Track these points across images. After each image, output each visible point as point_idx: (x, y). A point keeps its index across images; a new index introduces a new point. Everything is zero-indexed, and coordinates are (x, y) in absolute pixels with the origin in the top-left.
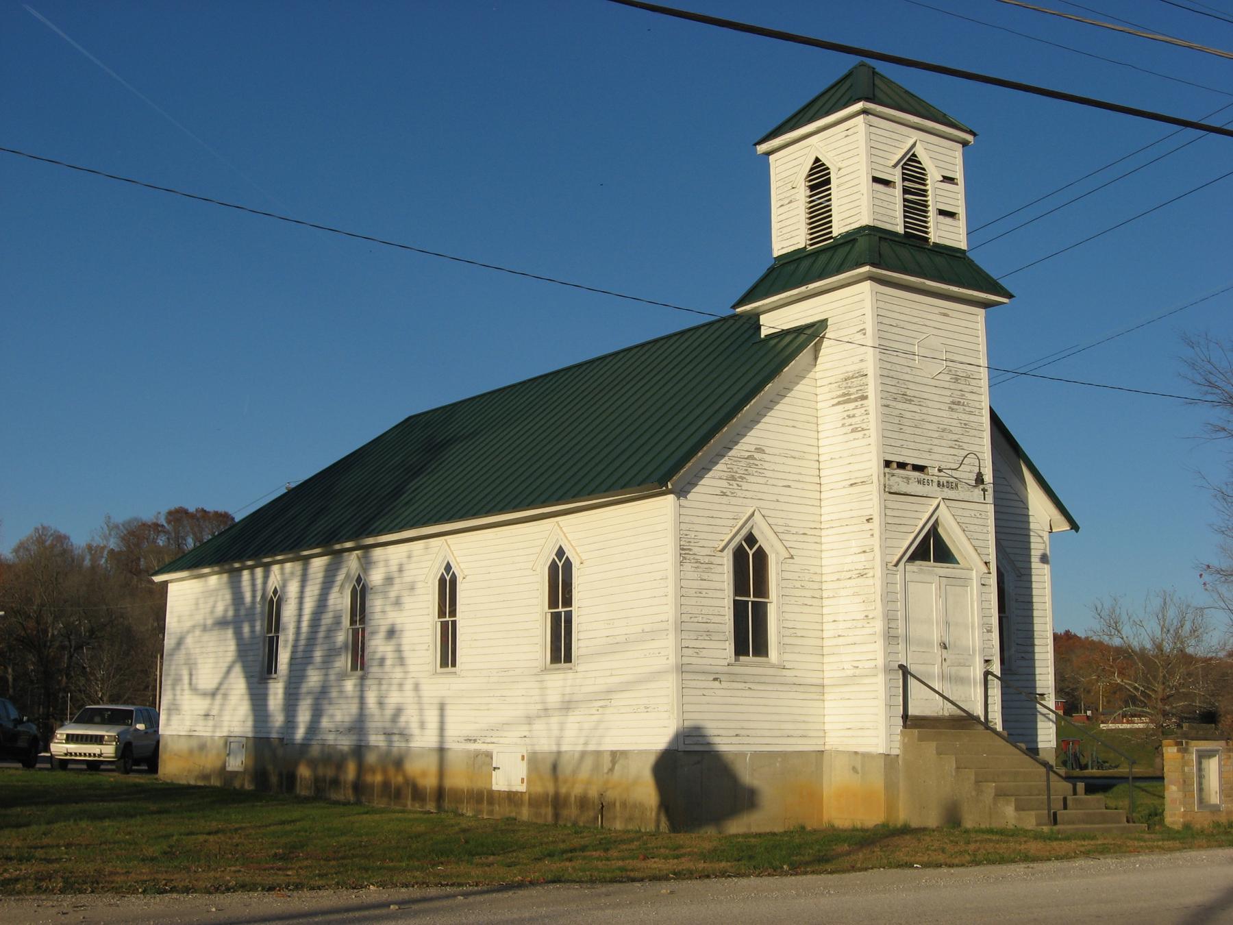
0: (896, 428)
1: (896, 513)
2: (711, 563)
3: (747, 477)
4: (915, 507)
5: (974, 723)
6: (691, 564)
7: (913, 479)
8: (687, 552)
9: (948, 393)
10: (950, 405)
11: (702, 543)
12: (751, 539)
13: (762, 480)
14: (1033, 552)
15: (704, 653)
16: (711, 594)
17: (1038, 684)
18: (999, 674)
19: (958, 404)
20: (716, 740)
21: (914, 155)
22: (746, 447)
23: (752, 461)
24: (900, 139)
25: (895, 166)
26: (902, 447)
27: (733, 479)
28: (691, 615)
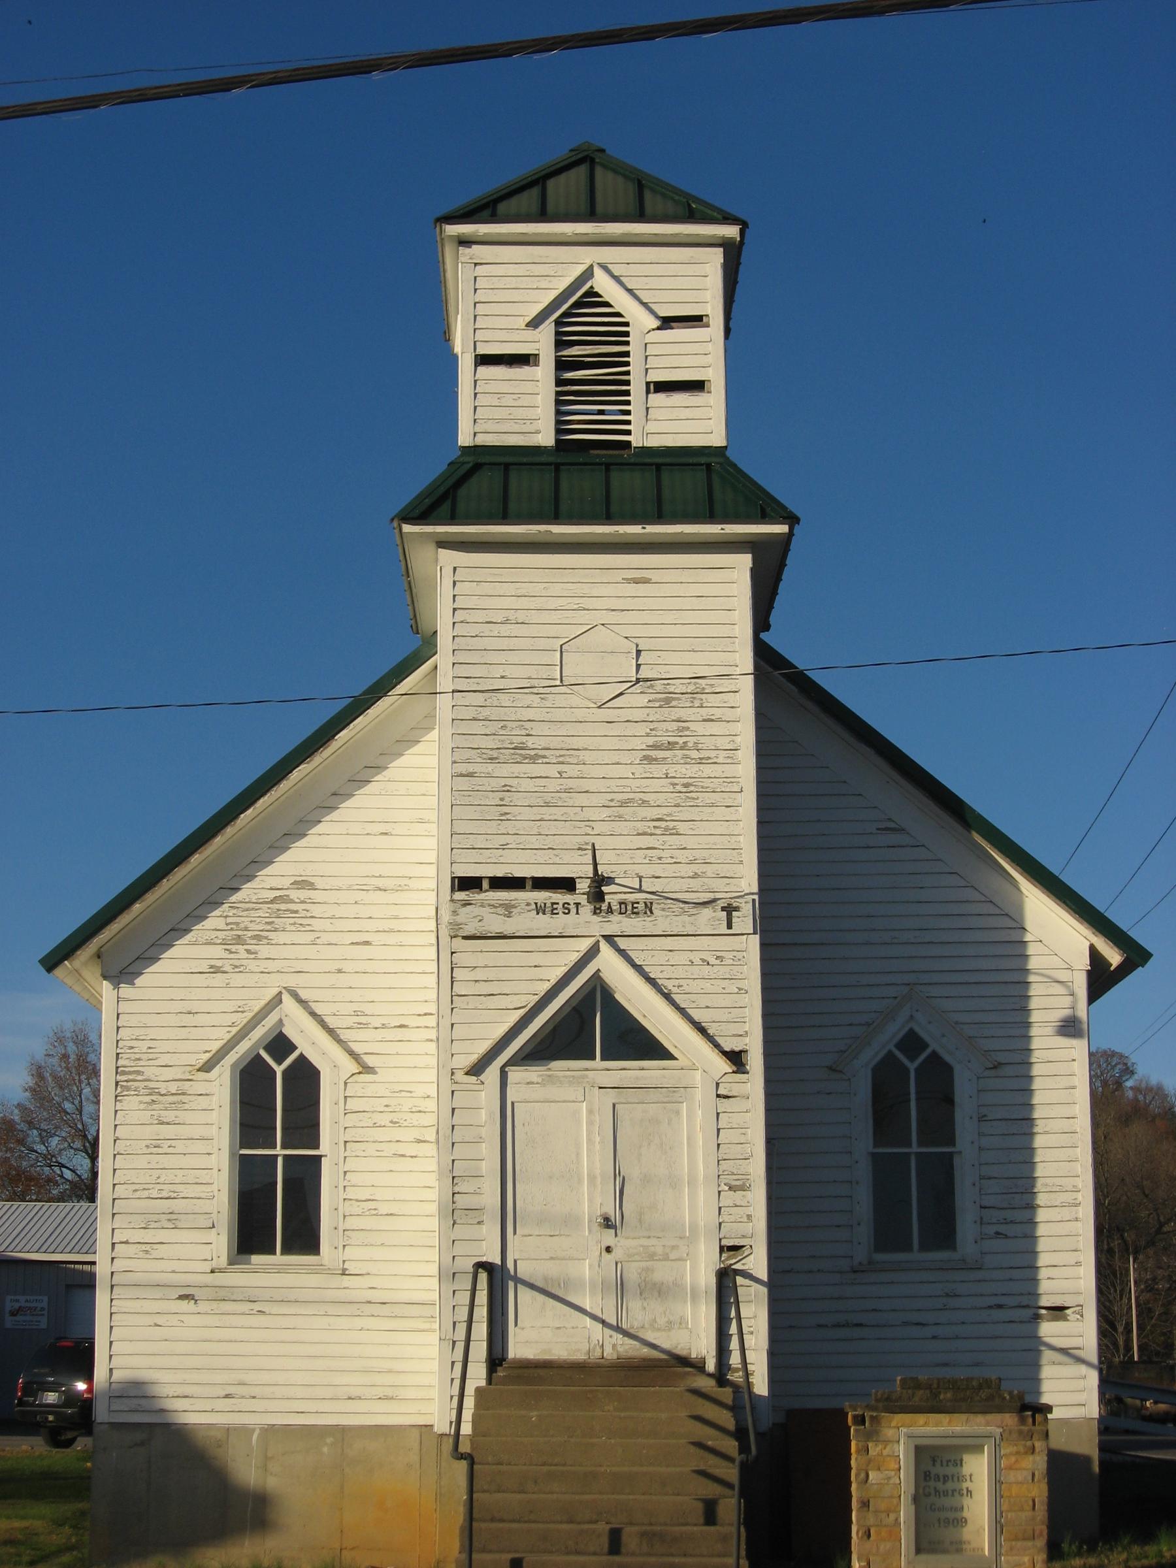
0: (494, 812)
1: (479, 974)
2: (184, 1094)
3: (271, 935)
4: (535, 959)
5: (688, 1373)
6: (140, 1098)
7: (523, 906)
8: (131, 1077)
9: (642, 729)
10: (645, 753)
11: (165, 1059)
12: (280, 1045)
13: (310, 937)
14: (1035, 1017)
15: (162, 1251)
16: (180, 1147)
17: (1045, 1286)
18: (763, 1274)
19: (671, 746)
21: (591, 293)
22: (275, 883)
23: (283, 907)
24: (552, 273)
25: (535, 323)
26: (504, 847)
27: (239, 940)
28: (137, 1187)
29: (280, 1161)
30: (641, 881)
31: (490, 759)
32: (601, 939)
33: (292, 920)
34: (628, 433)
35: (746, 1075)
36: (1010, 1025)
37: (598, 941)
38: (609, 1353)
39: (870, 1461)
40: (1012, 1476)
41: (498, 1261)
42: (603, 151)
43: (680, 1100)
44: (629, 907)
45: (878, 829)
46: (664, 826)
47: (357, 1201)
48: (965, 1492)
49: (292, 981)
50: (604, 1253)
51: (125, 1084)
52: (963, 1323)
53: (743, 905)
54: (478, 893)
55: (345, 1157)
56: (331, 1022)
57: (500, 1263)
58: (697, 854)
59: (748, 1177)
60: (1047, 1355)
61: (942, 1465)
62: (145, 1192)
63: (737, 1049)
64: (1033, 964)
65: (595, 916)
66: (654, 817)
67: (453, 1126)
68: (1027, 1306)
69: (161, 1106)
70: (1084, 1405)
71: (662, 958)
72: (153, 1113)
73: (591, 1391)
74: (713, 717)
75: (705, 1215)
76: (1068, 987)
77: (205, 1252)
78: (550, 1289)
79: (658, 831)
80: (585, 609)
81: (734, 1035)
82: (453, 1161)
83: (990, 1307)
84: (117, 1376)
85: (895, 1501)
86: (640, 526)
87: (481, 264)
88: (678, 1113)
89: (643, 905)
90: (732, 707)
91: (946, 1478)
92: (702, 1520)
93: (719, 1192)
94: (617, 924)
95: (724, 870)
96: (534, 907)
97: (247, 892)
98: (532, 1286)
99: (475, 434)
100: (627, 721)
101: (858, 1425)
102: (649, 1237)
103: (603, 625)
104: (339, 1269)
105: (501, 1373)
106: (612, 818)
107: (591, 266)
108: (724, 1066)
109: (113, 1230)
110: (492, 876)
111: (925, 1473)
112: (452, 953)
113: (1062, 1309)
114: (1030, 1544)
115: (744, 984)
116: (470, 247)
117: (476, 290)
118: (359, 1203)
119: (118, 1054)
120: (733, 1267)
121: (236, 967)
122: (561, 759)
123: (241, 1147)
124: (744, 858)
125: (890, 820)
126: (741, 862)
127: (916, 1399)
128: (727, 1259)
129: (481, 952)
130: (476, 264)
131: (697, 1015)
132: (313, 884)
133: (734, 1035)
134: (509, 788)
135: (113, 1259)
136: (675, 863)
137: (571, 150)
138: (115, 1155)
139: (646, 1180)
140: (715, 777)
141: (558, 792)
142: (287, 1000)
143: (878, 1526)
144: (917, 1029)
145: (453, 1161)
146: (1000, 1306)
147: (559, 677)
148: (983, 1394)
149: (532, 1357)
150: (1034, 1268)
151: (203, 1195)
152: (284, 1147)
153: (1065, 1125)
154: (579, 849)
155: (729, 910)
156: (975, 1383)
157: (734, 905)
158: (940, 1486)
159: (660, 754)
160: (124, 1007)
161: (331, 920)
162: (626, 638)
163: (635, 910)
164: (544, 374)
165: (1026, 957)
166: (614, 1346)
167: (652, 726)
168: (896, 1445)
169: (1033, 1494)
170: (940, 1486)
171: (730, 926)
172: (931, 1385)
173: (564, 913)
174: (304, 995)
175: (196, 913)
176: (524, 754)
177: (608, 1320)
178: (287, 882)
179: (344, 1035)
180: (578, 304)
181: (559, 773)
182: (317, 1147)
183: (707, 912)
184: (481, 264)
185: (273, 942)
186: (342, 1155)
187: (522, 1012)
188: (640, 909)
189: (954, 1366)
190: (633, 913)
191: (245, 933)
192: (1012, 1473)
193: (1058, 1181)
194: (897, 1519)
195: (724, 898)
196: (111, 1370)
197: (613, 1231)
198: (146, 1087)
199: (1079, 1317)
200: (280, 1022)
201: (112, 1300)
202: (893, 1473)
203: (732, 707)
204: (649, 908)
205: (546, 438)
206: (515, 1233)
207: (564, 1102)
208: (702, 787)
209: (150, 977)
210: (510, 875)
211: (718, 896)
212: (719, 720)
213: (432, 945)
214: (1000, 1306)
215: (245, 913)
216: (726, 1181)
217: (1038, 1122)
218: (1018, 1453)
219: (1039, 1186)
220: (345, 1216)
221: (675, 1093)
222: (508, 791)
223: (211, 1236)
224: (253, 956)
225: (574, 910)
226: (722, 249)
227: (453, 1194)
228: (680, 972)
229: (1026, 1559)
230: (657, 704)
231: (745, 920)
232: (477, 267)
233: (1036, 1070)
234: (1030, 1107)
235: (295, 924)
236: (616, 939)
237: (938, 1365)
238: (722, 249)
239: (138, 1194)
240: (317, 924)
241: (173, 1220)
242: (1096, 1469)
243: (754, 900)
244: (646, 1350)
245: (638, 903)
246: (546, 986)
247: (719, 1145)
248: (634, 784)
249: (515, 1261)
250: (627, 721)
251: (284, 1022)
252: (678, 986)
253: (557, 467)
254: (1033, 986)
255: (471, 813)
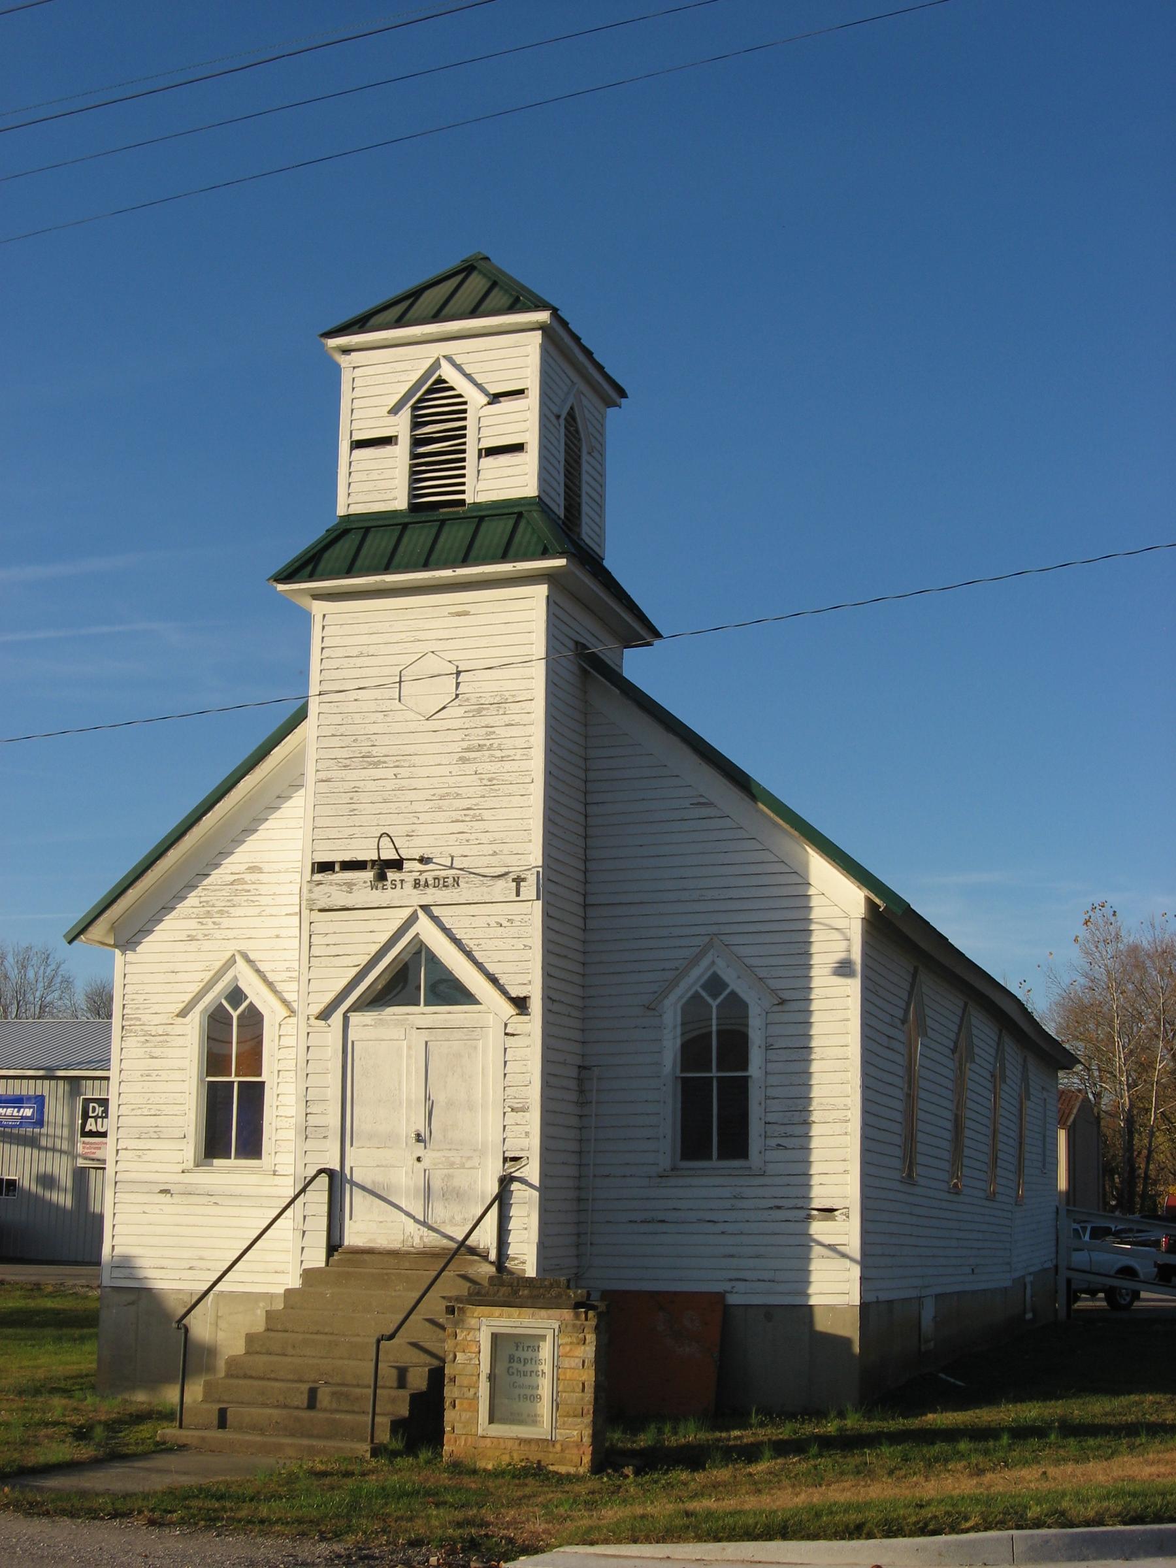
0: (345, 809)
1: (329, 940)
2: (167, 1035)
3: (231, 910)
4: (372, 925)
5: (475, 1261)
6: (139, 1039)
7: (361, 884)
8: (132, 1022)
9: (458, 735)
10: (461, 754)
11: (155, 1008)
12: (236, 995)
13: (257, 910)
14: (815, 960)
15: (150, 1156)
16: (164, 1075)
17: (816, 1192)
18: (536, 1181)
19: (480, 748)
20: (149, 1273)
21: (440, 381)
22: (235, 869)
23: (239, 887)
24: (410, 368)
25: (394, 410)
26: (351, 837)
27: (208, 915)
28: (134, 1107)
29: (236, 1085)
30: (452, 860)
31: (344, 766)
32: (418, 908)
33: (246, 898)
34: (463, 492)
35: (528, 1017)
36: (794, 967)
37: (416, 910)
38: (417, 1241)
39: (457, 1344)
40: (566, 1363)
41: (338, 1168)
42: (487, 259)
43: (478, 1037)
44: (441, 882)
45: (691, 804)
46: (472, 814)
47: (286, 1117)
48: (540, 1373)
49: (243, 946)
50: (416, 1162)
51: (128, 1027)
52: (748, 1221)
53: (529, 876)
54: (331, 874)
55: (278, 1083)
56: (271, 977)
57: (339, 1170)
58: (497, 835)
59: (527, 1100)
60: (817, 1250)
61: (523, 1350)
62: (140, 1110)
63: (522, 995)
64: (814, 915)
65: (415, 890)
66: (465, 808)
67: (308, 1061)
68: (802, 1208)
69: (152, 1045)
70: (848, 1294)
71: (466, 922)
72: (146, 1049)
73: (387, 1274)
74: (513, 722)
75: (493, 1135)
76: (843, 933)
77: (179, 1156)
78: (376, 1191)
79: (467, 819)
80: (419, 641)
81: (520, 984)
82: (307, 1088)
83: (771, 1208)
84: (117, 1251)
85: (475, 1378)
86: (451, 570)
87: (358, 367)
88: (475, 1048)
89: (452, 879)
90: (528, 713)
91: (526, 1361)
92: (395, 1384)
93: (504, 1113)
94: (431, 896)
95: (517, 848)
96: (369, 884)
97: (216, 876)
98: (363, 1188)
99: (349, 505)
100: (448, 730)
101: (449, 1314)
102: (450, 1150)
103: (433, 652)
104: (270, 1171)
105: (336, 1256)
106: (433, 810)
107: (438, 359)
108: (509, 1009)
109: (118, 1139)
110: (341, 860)
111: (510, 1356)
112: (311, 923)
113: (832, 1210)
114: (579, 1420)
115: (528, 942)
116: (350, 354)
117: (353, 389)
118: (286, 1119)
119: (124, 1005)
120: (513, 1175)
121: (206, 935)
122: (397, 764)
123: (207, 1076)
124: (533, 838)
125: (701, 796)
126: (530, 841)
127: (500, 1294)
128: (508, 1169)
129: (332, 921)
130: (354, 368)
131: (491, 968)
132: (261, 868)
133: (520, 984)
134: (356, 789)
135: (117, 1162)
136: (479, 844)
137: (463, 261)
138: (120, 1083)
139: (450, 1104)
140: (513, 772)
141: (393, 790)
142: (240, 962)
143: (461, 1398)
144: (719, 973)
145: (307, 1088)
146: (779, 1208)
147: (397, 697)
148: (553, 1293)
149: (362, 1245)
150: (808, 1176)
151: (178, 1113)
152: (237, 1075)
153: (839, 1052)
154: (407, 836)
155: (518, 881)
156: (546, 1283)
157: (522, 877)
158: (520, 1367)
159: (472, 755)
160: (129, 969)
161: (272, 897)
162: (450, 661)
163: (446, 884)
164: (400, 453)
165: (809, 908)
166: (421, 1237)
167: (467, 732)
168: (477, 1332)
169: (583, 1378)
170: (520, 1367)
171: (518, 895)
172: (512, 1283)
173: (392, 888)
174: (252, 956)
175: (179, 895)
176: (370, 761)
177: (417, 1217)
178: (243, 868)
179: (280, 987)
180: (429, 391)
181: (395, 775)
182: (260, 1075)
183: (501, 883)
184: (358, 367)
185: (232, 915)
186: (276, 1081)
187: (357, 969)
188: (450, 882)
189: (740, 1257)
190: (444, 886)
191: (213, 908)
192: (567, 1359)
193: (832, 1101)
194: (475, 1394)
195: (515, 871)
196: (113, 1246)
197: (423, 1144)
198: (142, 1030)
199: (844, 1217)
200: (236, 978)
201: (115, 1193)
202: (474, 1355)
203: (528, 713)
204: (456, 881)
205: (400, 502)
206: (352, 1145)
207: (390, 1040)
208: (503, 781)
209: (149, 945)
210: (355, 859)
211: (511, 869)
212: (518, 724)
213: (295, 914)
214: (779, 1208)
215: (213, 894)
216: (510, 1104)
217: (815, 1050)
218: (571, 1343)
219: (815, 1105)
220: (277, 1129)
221: (473, 1032)
222: (356, 792)
223: (182, 1144)
224: (217, 927)
225: (399, 886)
226: (540, 332)
227: (307, 1114)
228: (479, 933)
229: (575, 1433)
230: (471, 714)
231: (529, 889)
232: (355, 370)
233: (814, 1006)
234: (809, 1037)
235: (247, 900)
236: (432, 908)
237: (725, 1256)
238: (540, 332)
239: (134, 1113)
240: (264, 900)
241: (158, 1134)
242: (857, 1349)
243: (538, 872)
244: (445, 1241)
245: (448, 878)
246: (375, 948)
247: (505, 1074)
248: (451, 780)
249: (351, 1168)
250: (448, 730)
251: (239, 978)
252: (478, 945)
253: (405, 526)
254: (815, 934)
255: (328, 810)
